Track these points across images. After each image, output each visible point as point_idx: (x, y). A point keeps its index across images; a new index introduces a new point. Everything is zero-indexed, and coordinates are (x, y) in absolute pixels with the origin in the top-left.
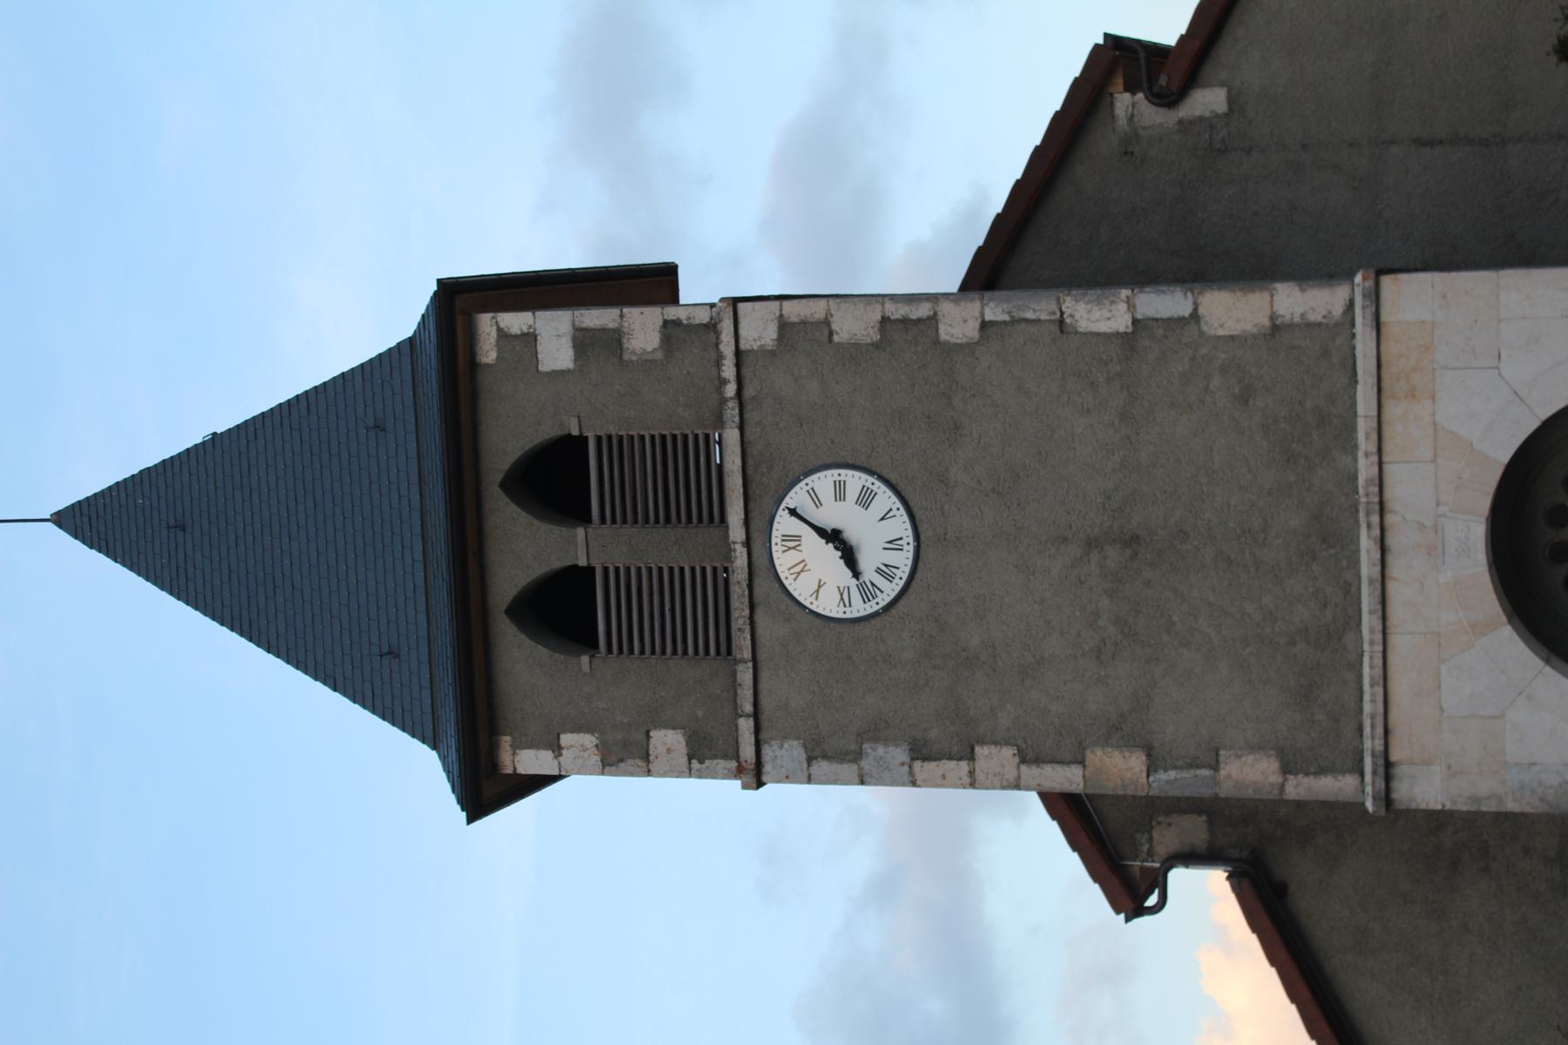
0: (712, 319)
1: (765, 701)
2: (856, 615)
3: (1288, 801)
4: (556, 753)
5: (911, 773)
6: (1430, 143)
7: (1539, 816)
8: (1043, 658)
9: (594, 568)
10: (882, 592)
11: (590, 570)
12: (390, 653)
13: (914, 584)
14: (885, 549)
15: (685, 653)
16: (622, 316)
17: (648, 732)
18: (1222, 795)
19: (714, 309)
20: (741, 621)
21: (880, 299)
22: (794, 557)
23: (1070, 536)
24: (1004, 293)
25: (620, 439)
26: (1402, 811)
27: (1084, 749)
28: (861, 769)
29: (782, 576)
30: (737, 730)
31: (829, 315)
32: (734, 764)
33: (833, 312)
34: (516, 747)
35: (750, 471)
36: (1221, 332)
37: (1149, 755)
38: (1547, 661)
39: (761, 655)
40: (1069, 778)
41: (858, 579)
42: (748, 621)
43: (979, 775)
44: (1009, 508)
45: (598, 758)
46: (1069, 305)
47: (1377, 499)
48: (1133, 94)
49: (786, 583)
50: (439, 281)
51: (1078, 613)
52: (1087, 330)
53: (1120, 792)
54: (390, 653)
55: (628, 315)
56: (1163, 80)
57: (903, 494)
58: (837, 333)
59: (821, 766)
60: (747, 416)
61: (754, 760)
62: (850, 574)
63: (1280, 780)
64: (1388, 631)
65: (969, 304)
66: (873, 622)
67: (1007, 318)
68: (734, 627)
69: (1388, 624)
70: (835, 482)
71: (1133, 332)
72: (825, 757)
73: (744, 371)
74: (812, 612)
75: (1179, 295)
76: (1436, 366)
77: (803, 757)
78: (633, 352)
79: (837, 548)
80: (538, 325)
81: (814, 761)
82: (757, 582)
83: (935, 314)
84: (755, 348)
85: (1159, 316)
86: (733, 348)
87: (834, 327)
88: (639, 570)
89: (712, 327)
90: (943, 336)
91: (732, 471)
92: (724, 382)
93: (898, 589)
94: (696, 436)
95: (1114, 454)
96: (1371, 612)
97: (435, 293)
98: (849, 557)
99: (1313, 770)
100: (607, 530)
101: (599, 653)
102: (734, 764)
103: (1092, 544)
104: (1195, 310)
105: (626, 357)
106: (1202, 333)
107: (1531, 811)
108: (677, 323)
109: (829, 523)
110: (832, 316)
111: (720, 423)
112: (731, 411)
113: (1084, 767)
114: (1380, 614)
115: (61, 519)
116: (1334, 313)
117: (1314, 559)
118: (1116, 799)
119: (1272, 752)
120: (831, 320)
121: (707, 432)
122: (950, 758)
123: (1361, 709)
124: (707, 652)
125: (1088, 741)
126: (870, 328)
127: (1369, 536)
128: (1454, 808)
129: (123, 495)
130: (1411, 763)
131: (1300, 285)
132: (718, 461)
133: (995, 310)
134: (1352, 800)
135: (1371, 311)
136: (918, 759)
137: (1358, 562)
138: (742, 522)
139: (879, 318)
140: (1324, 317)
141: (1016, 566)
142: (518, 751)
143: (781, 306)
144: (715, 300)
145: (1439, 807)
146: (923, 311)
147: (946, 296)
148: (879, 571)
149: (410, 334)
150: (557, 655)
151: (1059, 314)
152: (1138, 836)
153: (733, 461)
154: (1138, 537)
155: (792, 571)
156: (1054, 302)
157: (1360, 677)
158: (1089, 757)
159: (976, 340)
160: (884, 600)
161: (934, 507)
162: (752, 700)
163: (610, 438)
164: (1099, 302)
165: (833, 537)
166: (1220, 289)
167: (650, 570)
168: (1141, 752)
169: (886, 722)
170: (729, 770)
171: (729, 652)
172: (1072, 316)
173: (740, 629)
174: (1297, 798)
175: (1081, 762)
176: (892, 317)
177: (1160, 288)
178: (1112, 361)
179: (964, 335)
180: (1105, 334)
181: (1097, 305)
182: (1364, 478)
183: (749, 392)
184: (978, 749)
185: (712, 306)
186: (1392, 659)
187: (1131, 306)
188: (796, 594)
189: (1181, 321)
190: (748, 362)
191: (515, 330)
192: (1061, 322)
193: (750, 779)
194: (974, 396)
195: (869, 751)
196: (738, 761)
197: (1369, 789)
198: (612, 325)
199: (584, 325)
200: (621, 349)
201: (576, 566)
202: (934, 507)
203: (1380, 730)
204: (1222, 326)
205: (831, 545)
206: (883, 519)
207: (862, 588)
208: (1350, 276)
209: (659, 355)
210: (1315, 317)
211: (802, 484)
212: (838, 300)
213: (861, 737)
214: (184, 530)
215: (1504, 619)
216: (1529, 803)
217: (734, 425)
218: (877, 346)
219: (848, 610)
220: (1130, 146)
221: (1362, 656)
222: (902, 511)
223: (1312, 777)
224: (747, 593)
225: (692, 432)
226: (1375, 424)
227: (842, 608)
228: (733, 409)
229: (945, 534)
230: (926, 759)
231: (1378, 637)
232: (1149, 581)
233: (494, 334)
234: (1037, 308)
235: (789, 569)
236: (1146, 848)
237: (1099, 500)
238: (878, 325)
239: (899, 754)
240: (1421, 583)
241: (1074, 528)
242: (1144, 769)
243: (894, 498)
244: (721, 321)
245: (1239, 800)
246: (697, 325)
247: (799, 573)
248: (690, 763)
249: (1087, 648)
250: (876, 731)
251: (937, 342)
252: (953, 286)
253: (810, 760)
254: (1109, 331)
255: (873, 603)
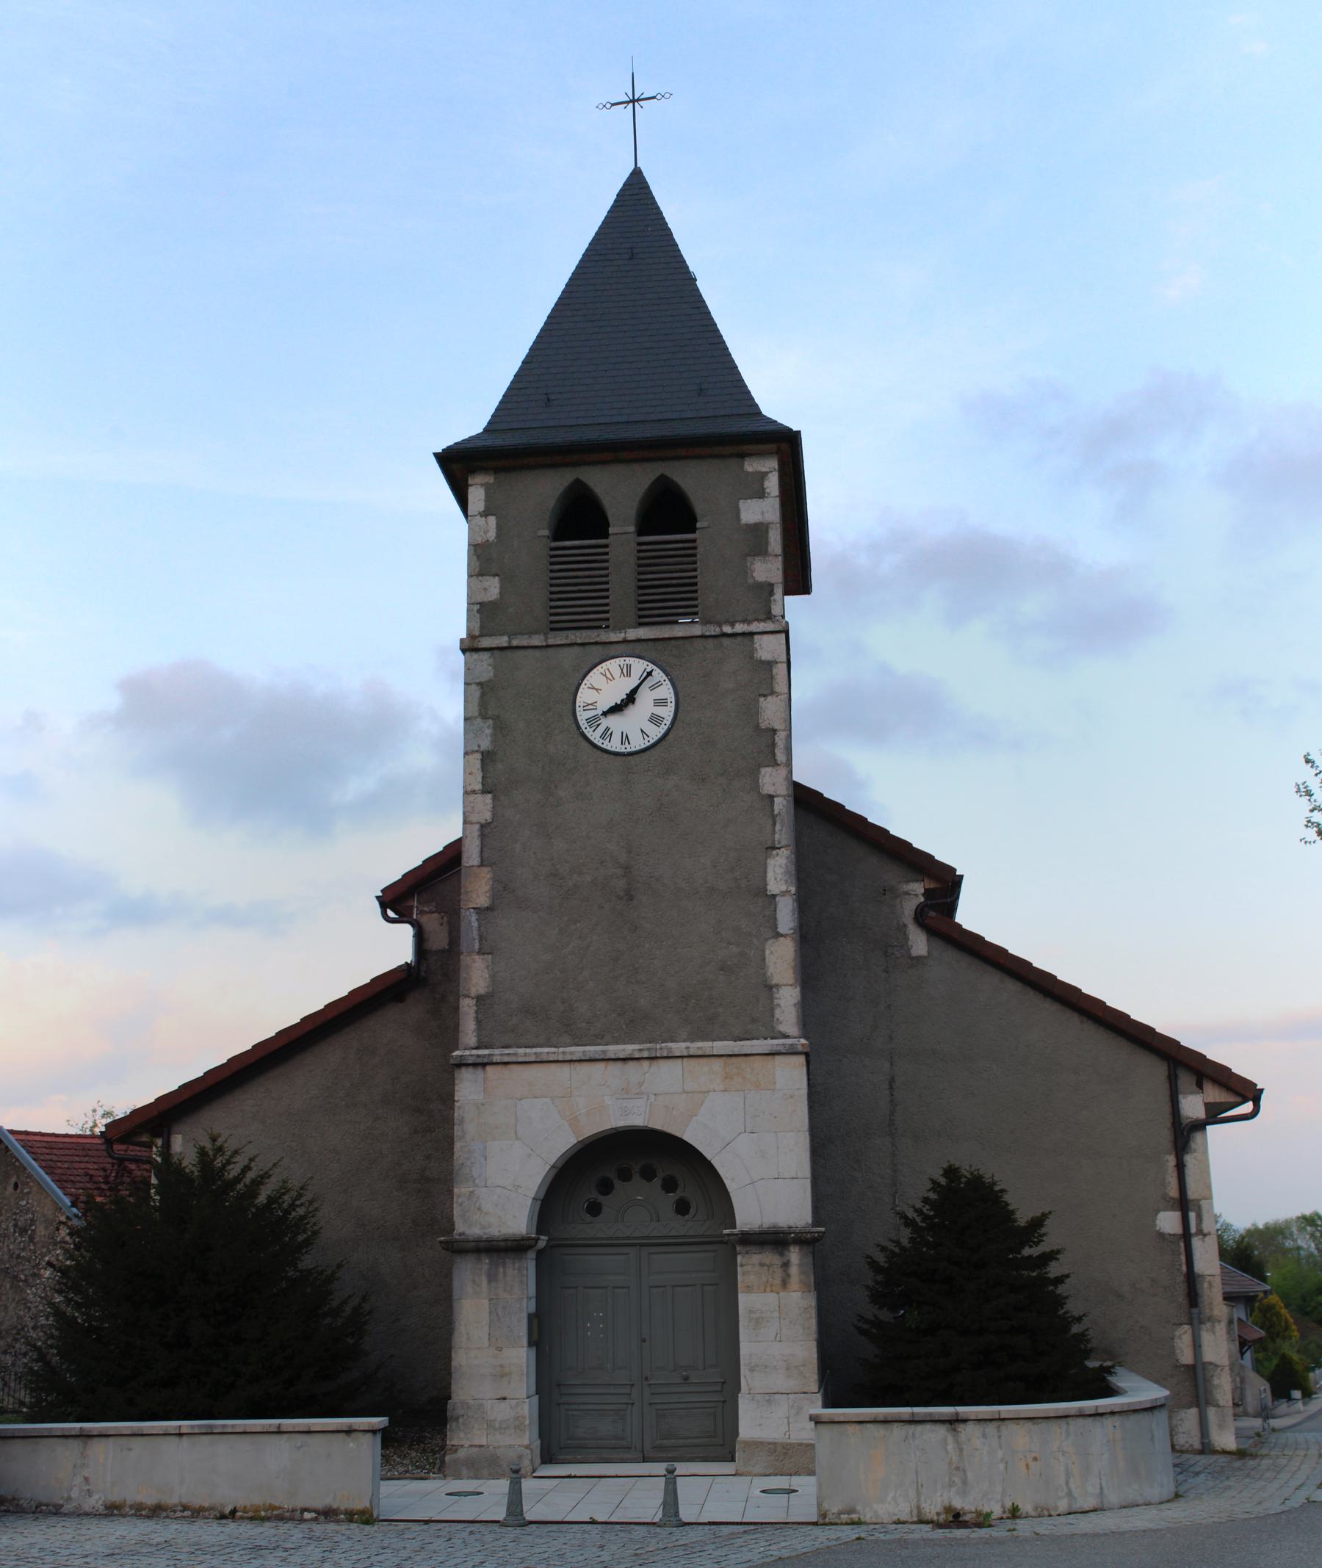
0: (775, 616)
1: (521, 653)
2: (578, 714)
3: (459, 1001)
4: (483, 514)
5: (473, 752)
6: (891, 1088)
7: (452, 1165)
8: (551, 838)
9: (607, 538)
10: (594, 731)
11: (606, 536)
12: (549, 400)
13: (600, 752)
14: (622, 733)
15: (551, 600)
16: (776, 556)
17: (497, 575)
18: (462, 957)
19: (781, 618)
20: (573, 637)
21: (788, 728)
22: (616, 672)
23: (632, 855)
24: (792, 811)
25: (694, 555)
26: (453, 1075)
27: (491, 866)
28: (476, 718)
29: (603, 665)
30: (500, 635)
31: (777, 694)
32: (477, 633)
33: (779, 697)
34: (487, 487)
35: (673, 642)
36: (767, 952)
37: (487, 909)
38: (553, 1167)
39: (550, 651)
40: (471, 857)
41: (601, 715)
42: (573, 642)
43: (472, 797)
44: (650, 815)
45: (479, 542)
46: (785, 852)
47: (658, 1055)
48: (923, 895)
49: (599, 667)
50: (799, 432)
51: (581, 861)
52: (768, 865)
53: (462, 890)
54: (549, 400)
55: (777, 560)
56: (932, 914)
57: (659, 745)
58: (765, 700)
59: (476, 692)
60: (710, 640)
61: (480, 647)
62: (605, 709)
63: (473, 995)
64: (572, 1064)
65: (785, 787)
66: (574, 726)
67: (776, 812)
68: (570, 633)
69: (577, 1064)
70: (667, 699)
71: (767, 895)
72: (483, 695)
73: (739, 639)
74: (580, 685)
75: (792, 925)
76: (746, 1092)
77: (482, 680)
78: (752, 564)
79: (622, 700)
80: (770, 499)
81: (480, 687)
82: (600, 647)
83: (779, 765)
84: (755, 646)
85: (778, 912)
86: (755, 631)
87: (769, 698)
88: (606, 568)
89: (769, 616)
90: (763, 770)
91: (673, 631)
92: (732, 625)
93: (596, 742)
94: (696, 606)
95: (687, 883)
96: (584, 1052)
97: (791, 430)
98: (616, 709)
99: (479, 1016)
100: (633, 546)
101: (551, 542)
102: (477, 633)
103: (627, 869)
104: (782, 935)
105: (749, 558)
106: (767, 940)
107: (455, 1158)
108: (771, 593)
109: (640, 697)
110: (777, 696)
111: (706, 622)
112: (713, 630)
113: (479, 866)
114: (584, 1058)
115: (637, 176)
116: (780, 1026)
117: (619, 1015)
118: (457, 890)
119: (491, 989)
120: (774, 696)
121: (699, 614)
122: (483, 778)
123: (521, 1047)
124: (552, 615)
125: (496, 869)
126: (768, 721)
127: (634, 1050)
128: (456, 1109)
129: (653, 217)
130: (485, 1080)
131: (798, 1003)
132: (680, 621)
133: (781, 804)
134: (460, 1042)
135: (782, 1049)
136: (483, 756)
137: (618, 1043)
138: (639, 637)
139: (776, 728)
140: (778, 1019)
141: (612, 820)
142: (483, 487)
143: (783, 662)
144: (787, 618)
145: (456, 1099)
146: (781, 757)
147: (791, 772)
148: (607, 729)
149: (764, 413)
150: (548, 514)
151: (778, 846)
152: (434, 904)
153: (680, 631)
154: (632, 900)
155: (607, 671)
156: (786, 843)
157: (541, 1046)
158: (486, 870)
159: (761, 792)
160: (589, 732)
161: (650, 765)
162: (521, 644)
163: (695, 548)
164: (787, 872)
165: (631, 698)
166: (796, 951)
167: (607, 576)
168: (489, 903)
169: (507, 734)
170: (473, 630)
171: (552, 629)
172: (778, 855)
173: (568, 636)
174: (461, 1006)
175: (482, 865)
176: (776, 736)
177: (796, 912)
178: (748, 881)
179: (765, 783)
180: (766, 877)
181: (785, 872)
182: (673, 1047)
183: (726, 641)
184: (490, 796)
185: (783, 617)
186: (553, 1066)
187: (784, 893)
188: (591, 674)
189: (775, 926)
190: (746, 640)
191: (766, 484)
192: (773, 848)
193: (467, 645)
194: (724, 791)
195: (488, 724)
196: (479, 636)
197: (467, 1053)
198: (770, 549)
199: (770, 531)
200: (754, 556)
201: (608, 526)
202: (650, 765)
203: (506, 1059)
204: (772, 953)
205: (625, 697)
206: (642, 731)
207: (596, 718)
208: (806, 1038)
209: (750, 581)
210: (777, 1012)
211: (665, 677)
212: (787, 700)
213: (496, 718)
214: (631, 259)
215: (580, 1139)
216: (460, 1156)
217: (704, 632)
218: (757, 726)
219: (582, 709)
220: (889, 893)
221: (555, 1047)
222: (648, 744)
223: (474, 1015)
224: (592, 641)
225: (699, 604)
226: (707, 1053)
227: (582, 705)
228: (715, 631)
229: (632, 773)
230: (482, 761)
231: (568, 1058)
232: (603, 908)
233: (764, 470)
234: (783, 832)
235: (608, 669)
236: (426, 909)
237: (656, 873)
238: (771, 727)
239: (486, 744)
240: (604, 1085)
241: (637, 858)
242: (478, 906)
243: (656, 739)
244: (773, 622)
245: (459, 969)
246: (770, 607)
247: (605, 676)
248: (477, 604)
249: (558, 867)
250: (501, 728)
251: (760, 766)
252: (795, 778)
253: (480, 684)
254: (768, 879)
255: (586, 725)
